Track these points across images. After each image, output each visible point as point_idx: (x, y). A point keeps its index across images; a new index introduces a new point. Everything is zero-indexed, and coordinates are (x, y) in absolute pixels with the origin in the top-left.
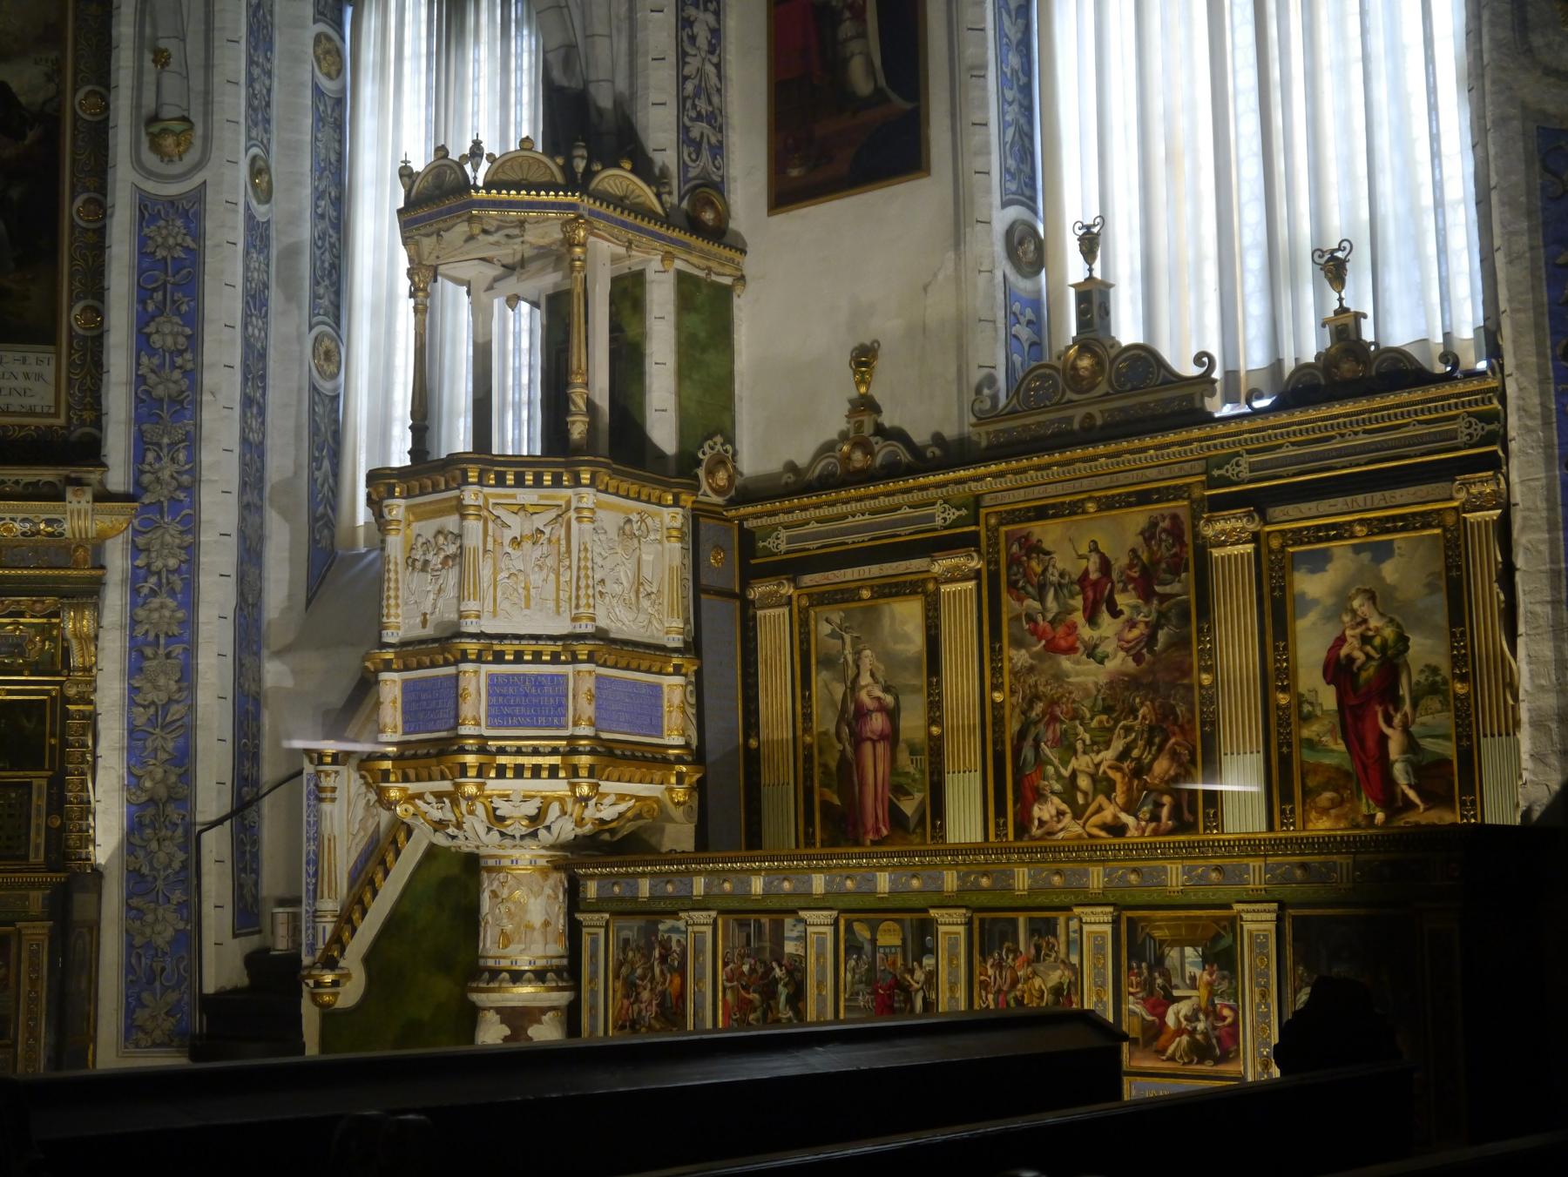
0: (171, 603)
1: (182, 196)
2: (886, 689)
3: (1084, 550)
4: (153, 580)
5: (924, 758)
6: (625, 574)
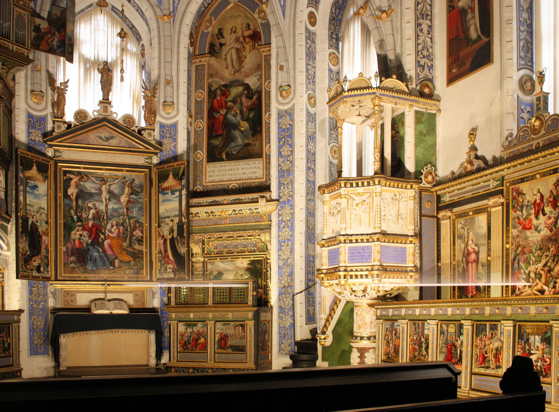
1: (289, 109)
5: (486, 268)
6: (394, 212)
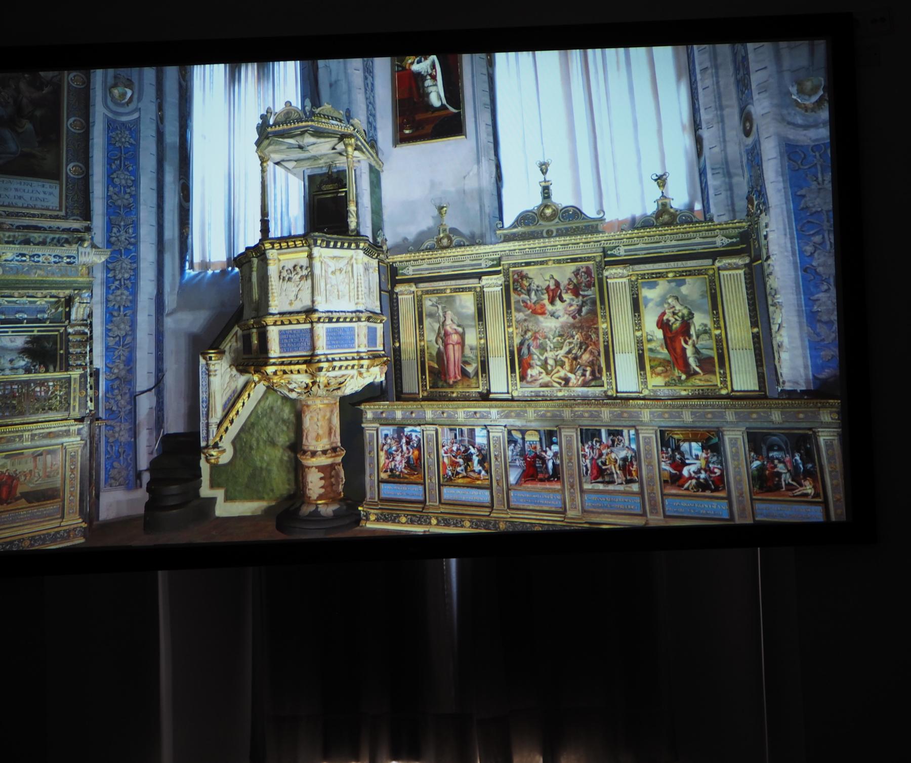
0: (126, 293)
2: (459, 326)
3: (547, 277)
4: (117, 283)
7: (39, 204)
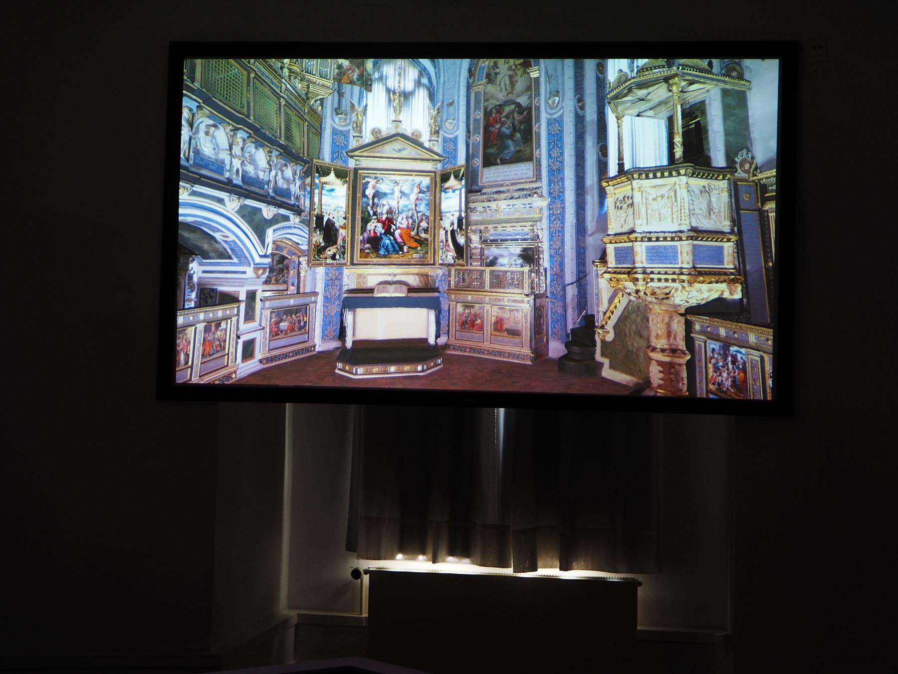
6: (704, 206)
7: (524, 176)
